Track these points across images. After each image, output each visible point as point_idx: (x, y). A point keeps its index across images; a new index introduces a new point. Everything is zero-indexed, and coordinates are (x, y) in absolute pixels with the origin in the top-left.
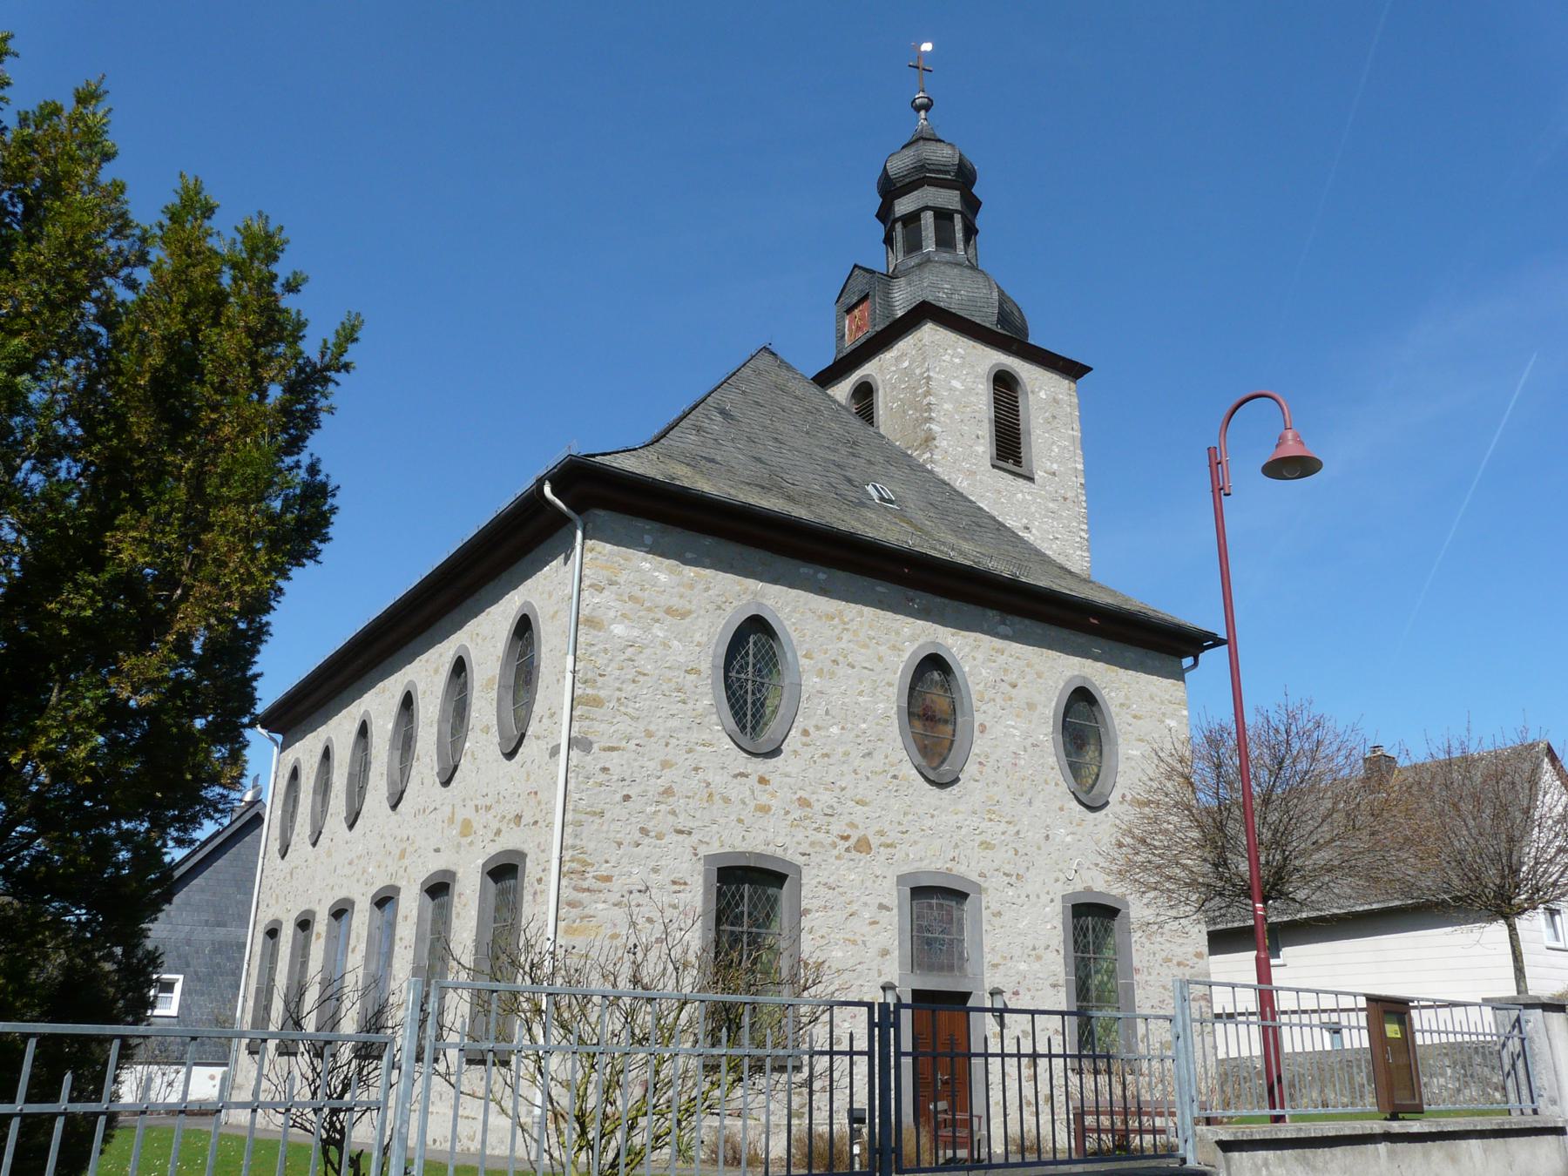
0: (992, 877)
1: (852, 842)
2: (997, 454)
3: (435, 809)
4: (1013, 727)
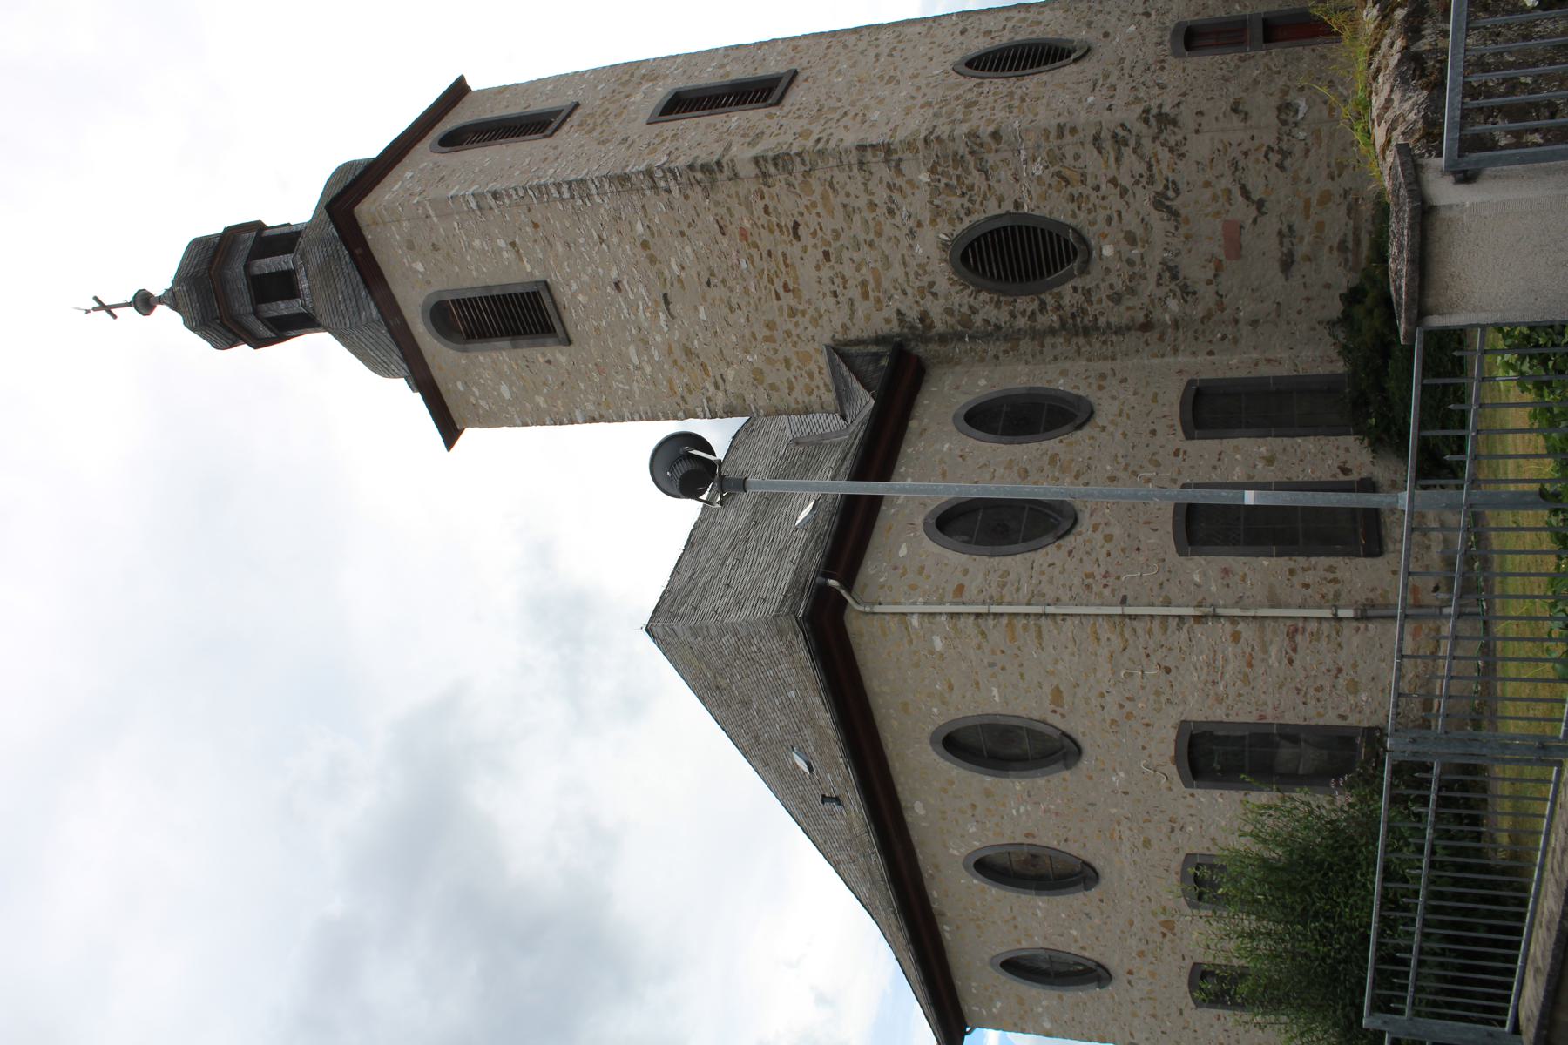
0: (1177, 843)
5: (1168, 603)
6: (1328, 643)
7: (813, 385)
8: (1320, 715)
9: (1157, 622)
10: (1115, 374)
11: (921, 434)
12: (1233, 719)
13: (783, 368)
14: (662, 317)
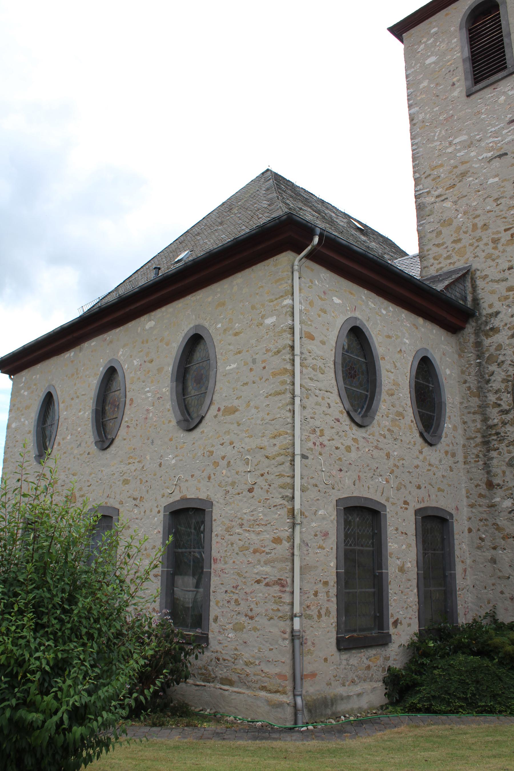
5: (303, 490)
6: (272, 609)
7: (441, 260)
8: (217, 603)
9: (289, 480)
10: (455, 463)
11: (414, 325)
12: (214, 540)
13: (453, 238)
14: (490, 154)
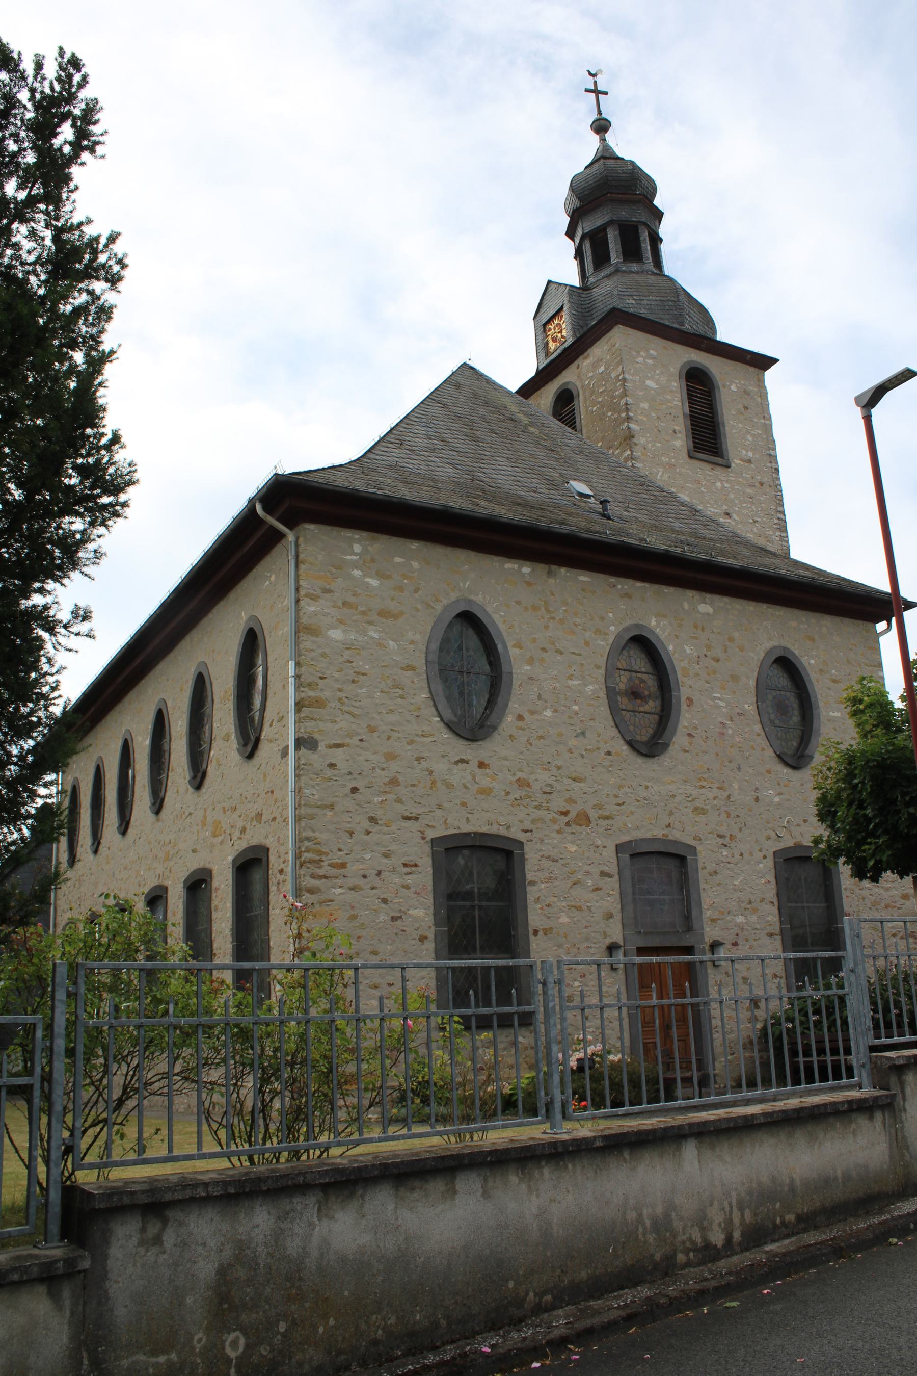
1: (573, 815)
2: (694, 447)
3: (190, 814)
4: (719, 699)
12: (844, 894)
